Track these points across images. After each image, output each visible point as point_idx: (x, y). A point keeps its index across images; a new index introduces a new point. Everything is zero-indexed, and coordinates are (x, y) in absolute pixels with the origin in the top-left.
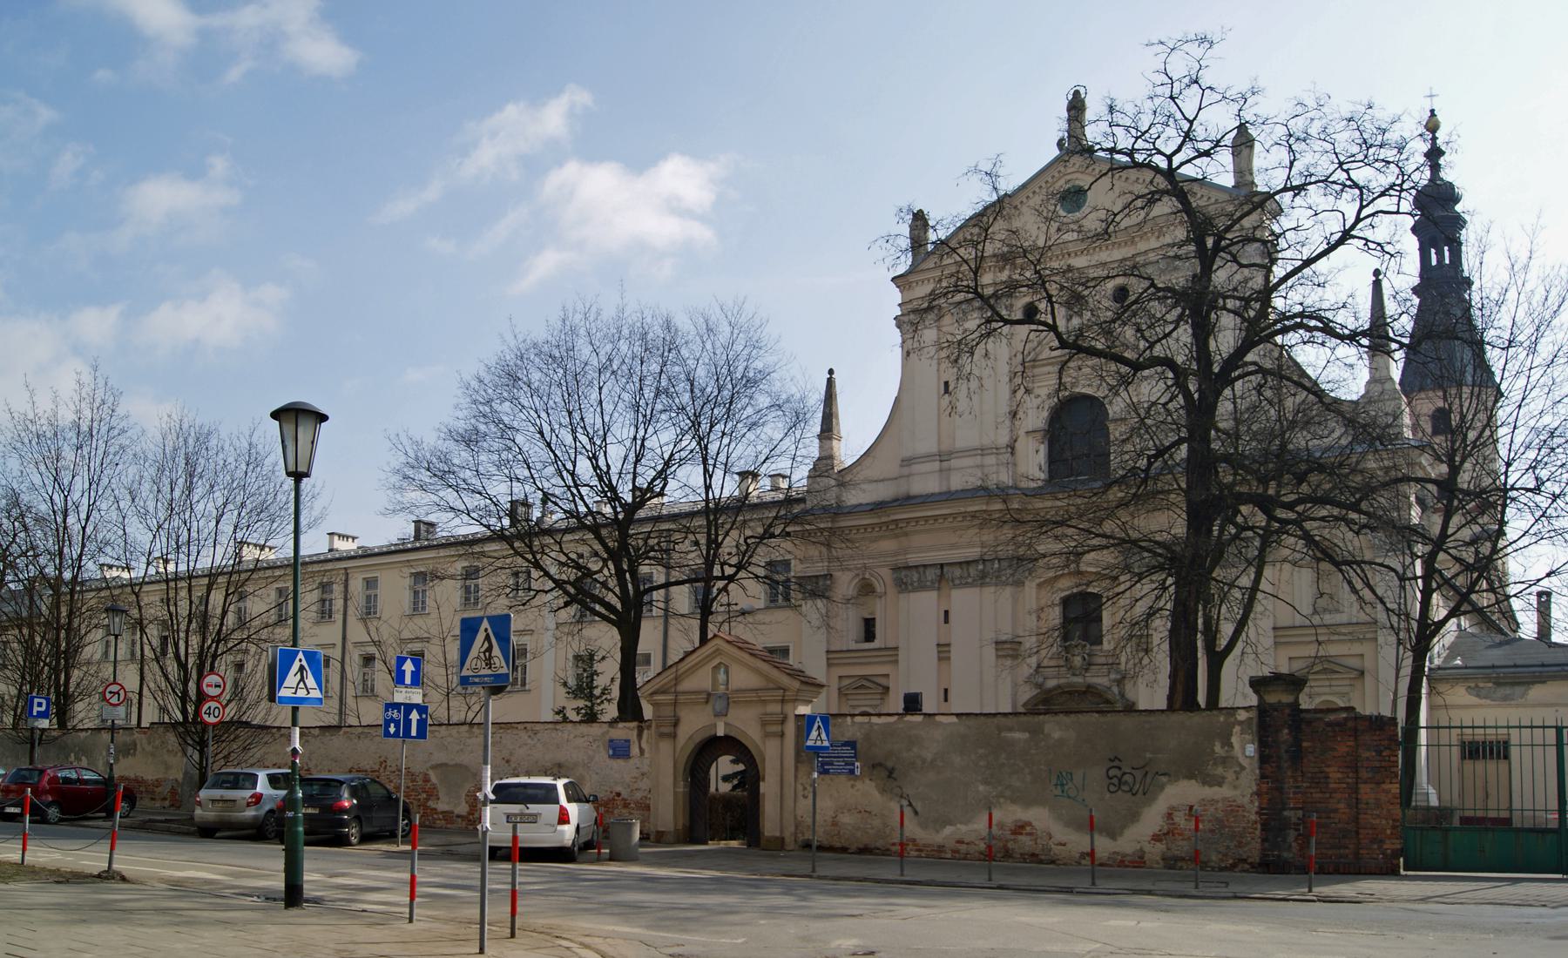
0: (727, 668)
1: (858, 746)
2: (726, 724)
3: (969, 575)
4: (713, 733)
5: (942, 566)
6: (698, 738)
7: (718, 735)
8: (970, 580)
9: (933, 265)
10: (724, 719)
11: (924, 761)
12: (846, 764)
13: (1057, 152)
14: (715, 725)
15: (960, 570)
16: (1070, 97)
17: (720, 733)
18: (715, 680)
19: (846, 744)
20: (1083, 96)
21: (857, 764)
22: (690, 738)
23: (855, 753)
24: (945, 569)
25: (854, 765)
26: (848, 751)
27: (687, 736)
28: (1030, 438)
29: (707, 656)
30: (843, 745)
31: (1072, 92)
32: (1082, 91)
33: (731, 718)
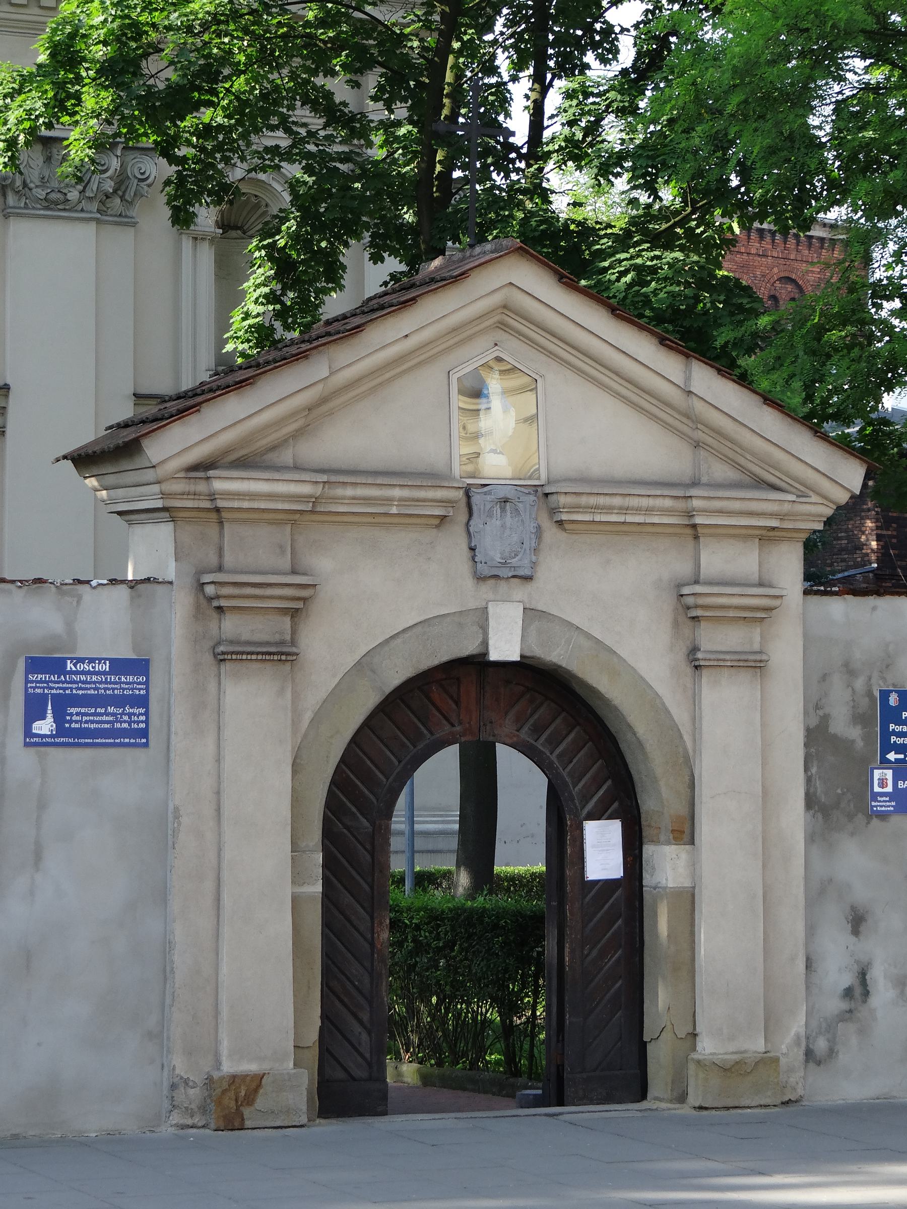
2: (531, 614)
4: (469, 648)
7: (494, 656)
10: (520, 592)
14: (482, 618)
22: (359, 665)
27: (350, 660)
29: (455, 330)
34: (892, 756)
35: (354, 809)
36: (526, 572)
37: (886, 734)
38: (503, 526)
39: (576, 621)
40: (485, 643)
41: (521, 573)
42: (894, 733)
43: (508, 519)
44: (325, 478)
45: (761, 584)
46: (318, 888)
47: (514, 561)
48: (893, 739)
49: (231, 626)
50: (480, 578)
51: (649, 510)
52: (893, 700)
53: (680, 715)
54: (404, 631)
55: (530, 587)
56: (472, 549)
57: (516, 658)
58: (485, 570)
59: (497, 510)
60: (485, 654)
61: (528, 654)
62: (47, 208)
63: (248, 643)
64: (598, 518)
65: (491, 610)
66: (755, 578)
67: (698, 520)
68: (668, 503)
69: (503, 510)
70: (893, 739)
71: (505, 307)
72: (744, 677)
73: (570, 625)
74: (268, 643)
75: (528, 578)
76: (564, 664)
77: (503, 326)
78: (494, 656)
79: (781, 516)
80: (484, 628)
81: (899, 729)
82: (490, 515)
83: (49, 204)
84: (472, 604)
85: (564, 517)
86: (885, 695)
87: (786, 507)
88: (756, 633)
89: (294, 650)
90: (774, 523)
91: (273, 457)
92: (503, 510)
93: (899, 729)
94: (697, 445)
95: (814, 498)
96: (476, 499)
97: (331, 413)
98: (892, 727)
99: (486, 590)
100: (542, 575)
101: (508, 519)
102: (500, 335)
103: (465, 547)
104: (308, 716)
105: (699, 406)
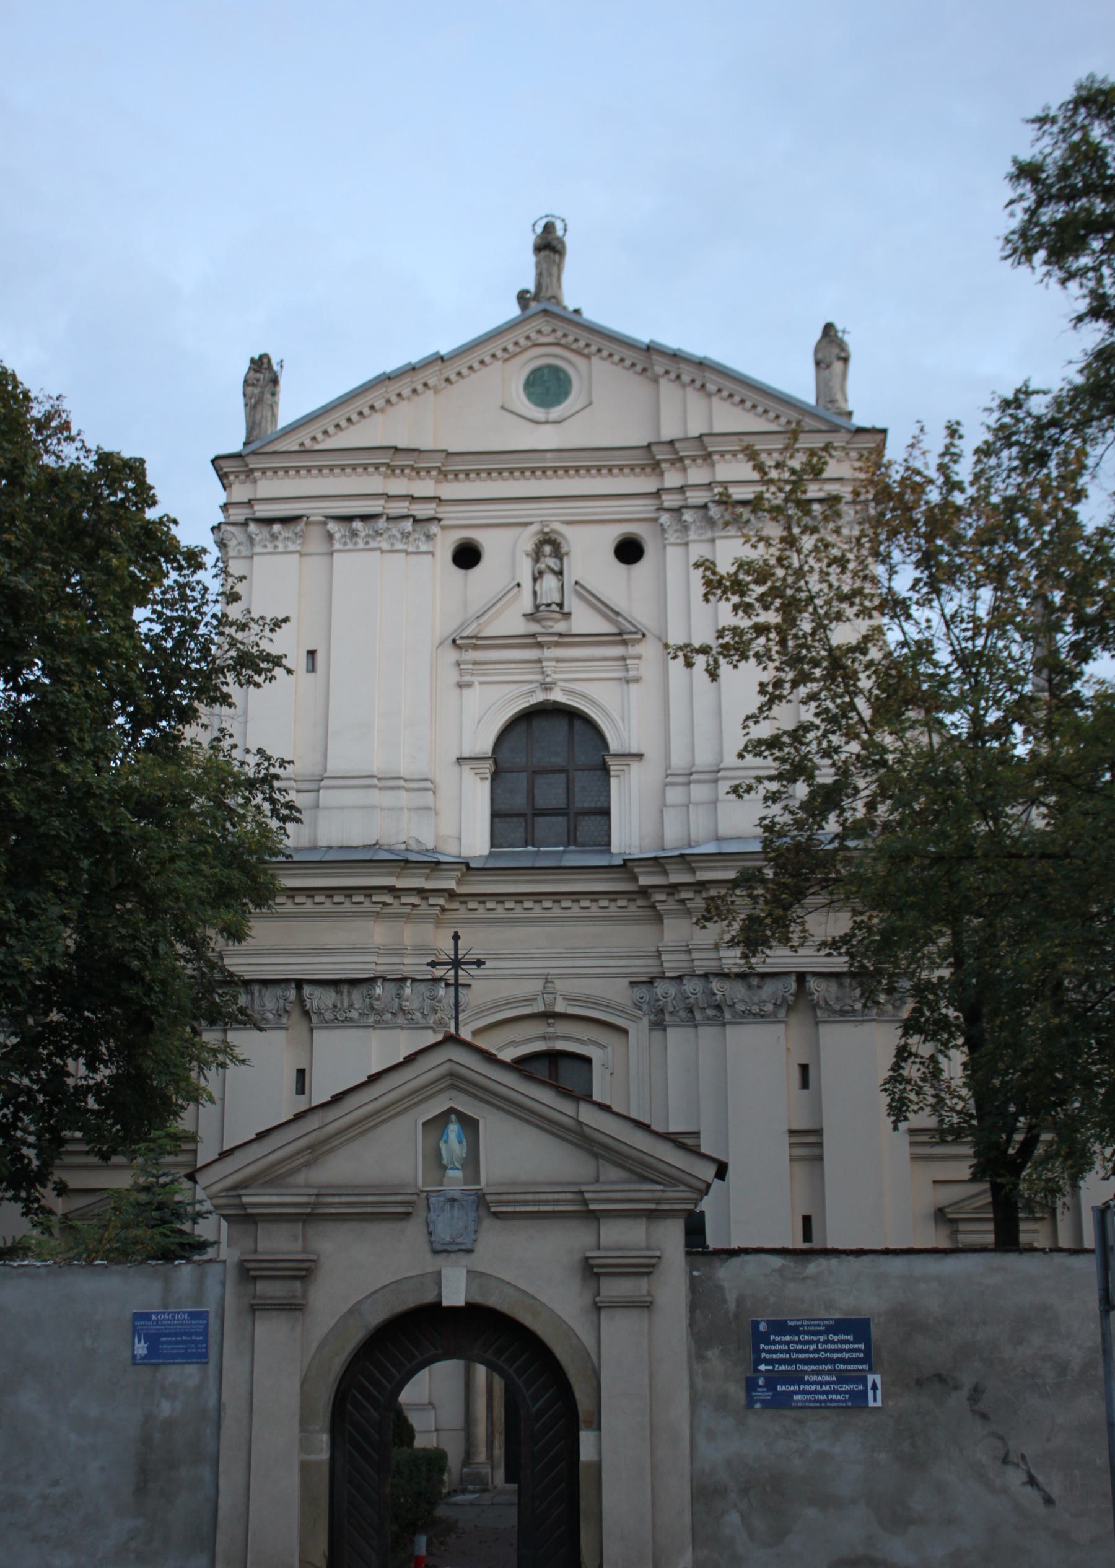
0: (470, 1125)
1: (875, 1332)
2: (473, 1274)
3: (351, 1005)
4: (429, 1298)
5: (299, 984)
6: (376, 1316)
8: (354, 1014)
9: (296, 448)
10: (464, 1259)
11: (1063, 1368)
12: (841, 1380)
13: (513, 311)
14: (437, 1278)
15: (333, 994)
16: (539, 229)
17: (455, 1295)
18: (436, 1163)
19: (840, 1326)
20: (560, 233)
21: (870, 1378)
22: (351, 1312)
23: (867, 1351)
24: (307, 990)
25: (864, 1381)
26: (845, 1345)
27: (345, 1308)
28: (466, 769)
30: (830, 1330)
31: (542, 223)
32: (559, 226)
33: (481, 1260)
34: (763, 1367)
35: (367, 1405)
36: (469, 1246)
37: (757, 1351)
38: (452, 1217)
39: (507, 1279)
40: (440, 1295)
41: (463, 1247)
42: (764, 1350)
43: (456, 1212)
44: (315, 1191)
45: (648, 1249)
46: (325, 1456)
47: (459, 1240)
48: (763, 1355)
49: (262, 1287)
50: (436, 1252)
51: (556, 1202)
52: (762, 1327)
53: (588, 1340)
54: (383, 1287)
55: (472, 1256)
56: (430, 1234)
57: (462, 1303)
58: (438, 1247)
59: (448, 1207)
60: (440, 1303)
61: (471, 1301)
62: (842, 1016)
63: (270, 1298)
64: (518, 1209)
65: (443, 1273)
66: (643, 1244)
67: (592, 1207)
68: (569, 1196)
69: (452, 1207)
70: (763, 1355)
71: (451, 1075)
72: (634, 1313)
73: (502, 1281)
74: (285, 1298)
75: (470, 1251)
76: (498, 1307)
77: (453, 1087)
78: (445, 1303)
79: (658, 1201)
80: (439, 1285)
81: (767, 1347)
82: (442, 1210)
83: (842, 1013)
84: (430, 1270)
85: (493, 1209)
86: (755, 1324)
87: (658, 1195)
88: (643, 1284)
89: (304, 1302)
90: (652, 1206)
91: (291, 1180)
92: (452, 1207)
93: (767, 1347)
94: (596, 1156)
95: (682, 1188)
96: (433, 1200)
97: (332, 1150)
98: (762, 1346)
99: (441, 1260)
100: (480, 1248)
101: (456, 1212)
102: (453, 1093)
103: (426, 1232)
104: (314, 1345)
105: (586, 1129)
